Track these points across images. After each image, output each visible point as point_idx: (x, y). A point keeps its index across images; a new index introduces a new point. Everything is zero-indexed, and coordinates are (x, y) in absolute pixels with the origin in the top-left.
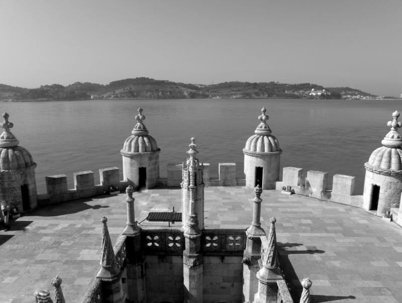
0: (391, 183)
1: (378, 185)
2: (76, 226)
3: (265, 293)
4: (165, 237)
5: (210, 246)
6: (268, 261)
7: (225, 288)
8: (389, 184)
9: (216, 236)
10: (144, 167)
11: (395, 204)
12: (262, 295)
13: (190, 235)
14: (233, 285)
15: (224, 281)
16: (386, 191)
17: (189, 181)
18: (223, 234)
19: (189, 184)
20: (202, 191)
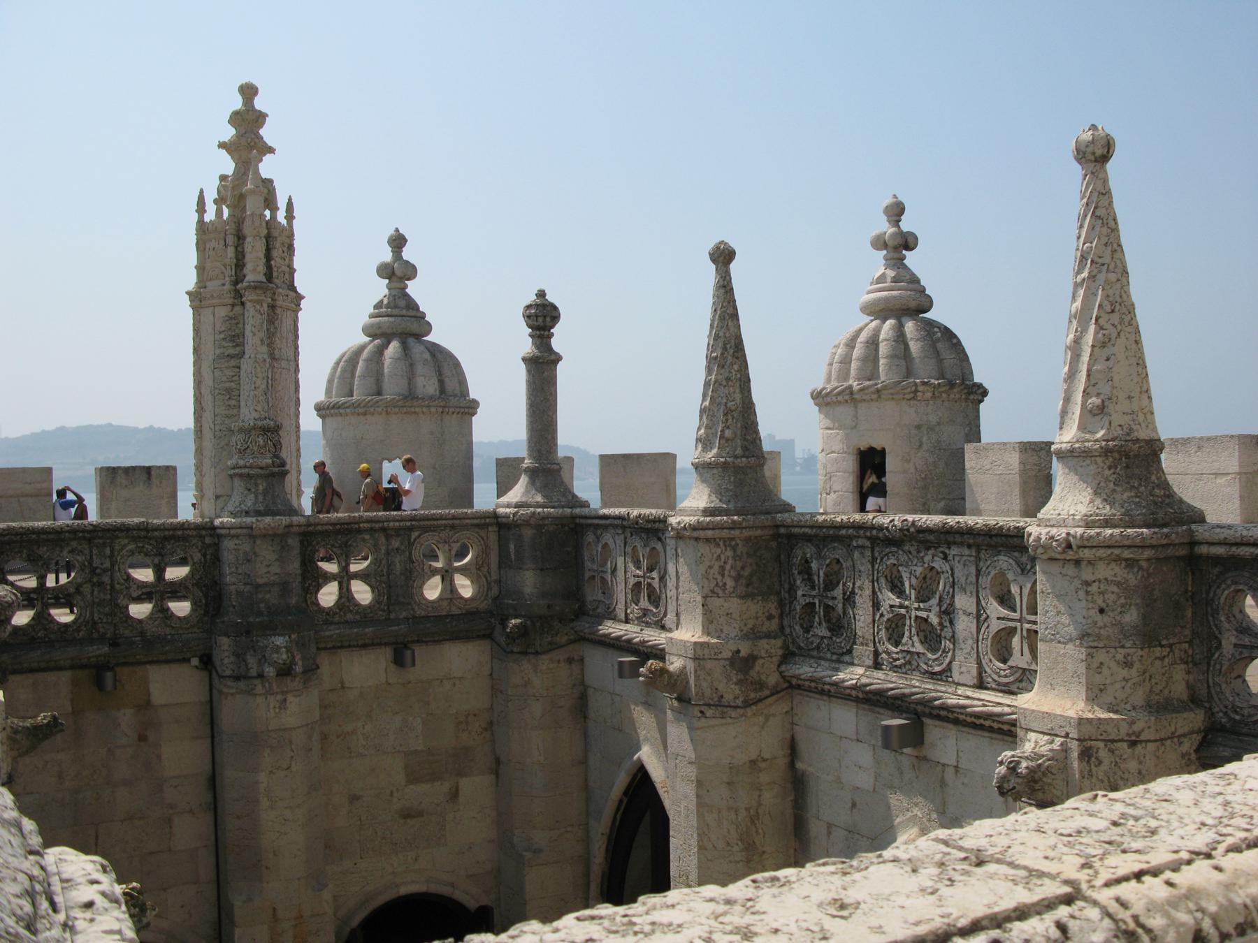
0: (918, 427)
1: (877, 444)
3: (730, 583)
4: (112, 565)
6: (728, 433)
7: (420, 814)
8: (914, 432)
11: (942, 504)
12: (715, 602)
13: (258, 513)
14: (454, 795)
15: (413, 777)
16: (908, 461)
17: (240, 264)
19: (238, 280)
20: (290, 322)
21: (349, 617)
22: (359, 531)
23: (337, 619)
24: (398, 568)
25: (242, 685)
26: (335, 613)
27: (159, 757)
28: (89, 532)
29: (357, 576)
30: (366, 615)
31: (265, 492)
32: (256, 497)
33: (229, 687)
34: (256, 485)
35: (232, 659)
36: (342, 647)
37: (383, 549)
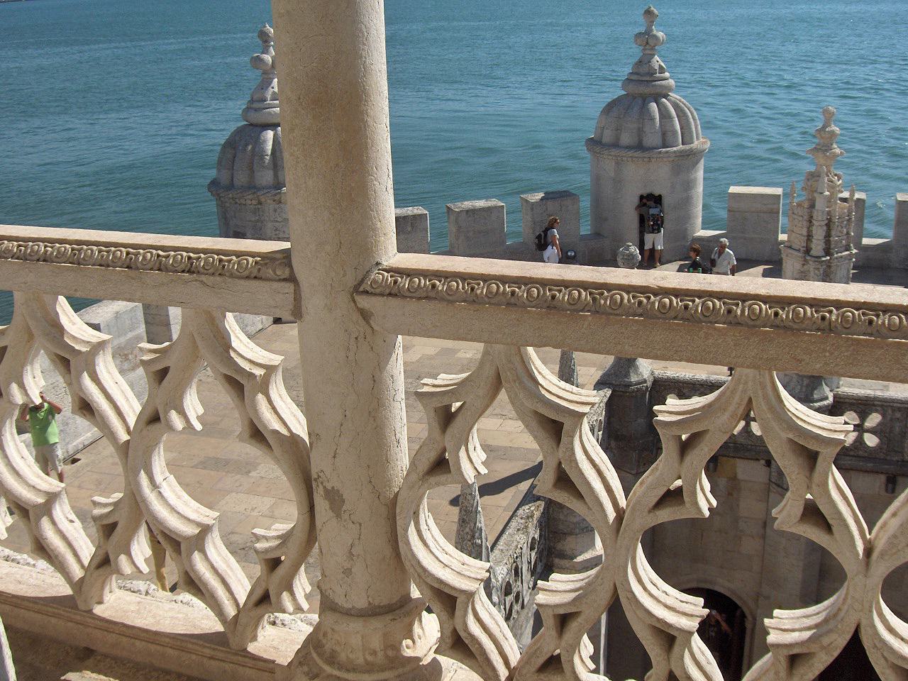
2: (460, 355)
5: (855, 441)
9: (876, 411)
10: (657, 193)
18: (899, 409)
19: (808, 251)
21: (861, 453)
22: (874, 405)
23: (852, 453)
24: (897, 429)
25: (780, 489)
26: (851, 450)
27: (738, 505)
28: (710, 386)
29: (868, 431)
30: (871, 455)
31: (808, 386)
32: (801, 388)
33: (774, 488)
34: (803, 381)
35: (776, 474)
36: (852, 470)
37: (889, 417)
